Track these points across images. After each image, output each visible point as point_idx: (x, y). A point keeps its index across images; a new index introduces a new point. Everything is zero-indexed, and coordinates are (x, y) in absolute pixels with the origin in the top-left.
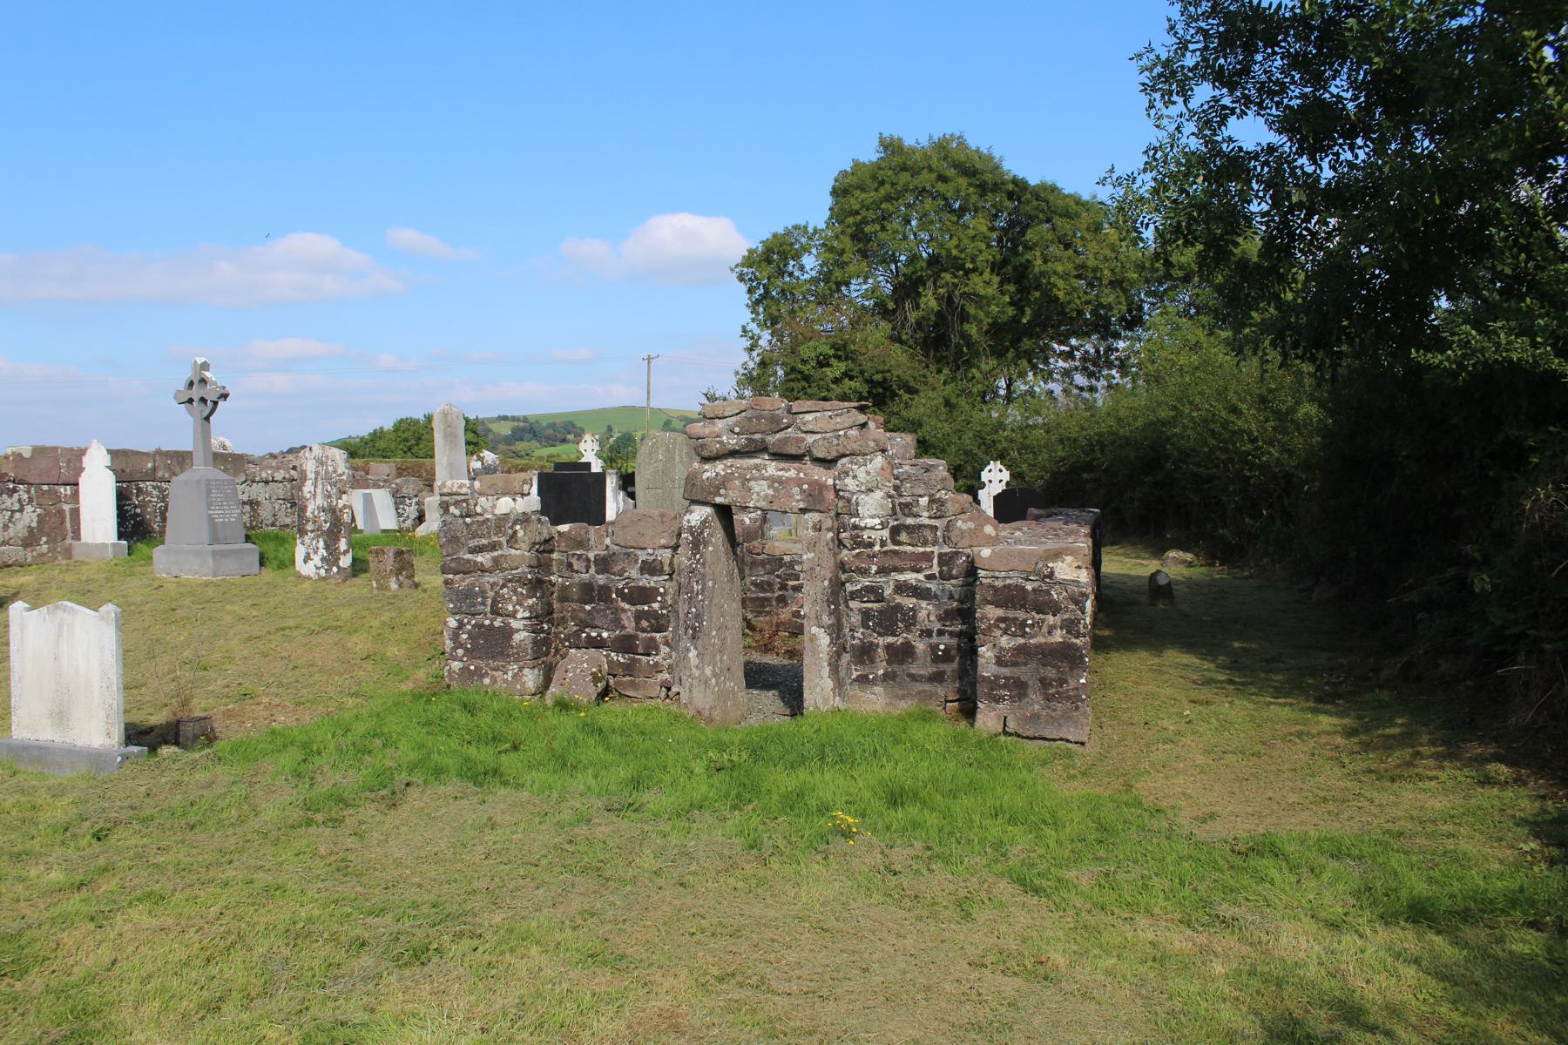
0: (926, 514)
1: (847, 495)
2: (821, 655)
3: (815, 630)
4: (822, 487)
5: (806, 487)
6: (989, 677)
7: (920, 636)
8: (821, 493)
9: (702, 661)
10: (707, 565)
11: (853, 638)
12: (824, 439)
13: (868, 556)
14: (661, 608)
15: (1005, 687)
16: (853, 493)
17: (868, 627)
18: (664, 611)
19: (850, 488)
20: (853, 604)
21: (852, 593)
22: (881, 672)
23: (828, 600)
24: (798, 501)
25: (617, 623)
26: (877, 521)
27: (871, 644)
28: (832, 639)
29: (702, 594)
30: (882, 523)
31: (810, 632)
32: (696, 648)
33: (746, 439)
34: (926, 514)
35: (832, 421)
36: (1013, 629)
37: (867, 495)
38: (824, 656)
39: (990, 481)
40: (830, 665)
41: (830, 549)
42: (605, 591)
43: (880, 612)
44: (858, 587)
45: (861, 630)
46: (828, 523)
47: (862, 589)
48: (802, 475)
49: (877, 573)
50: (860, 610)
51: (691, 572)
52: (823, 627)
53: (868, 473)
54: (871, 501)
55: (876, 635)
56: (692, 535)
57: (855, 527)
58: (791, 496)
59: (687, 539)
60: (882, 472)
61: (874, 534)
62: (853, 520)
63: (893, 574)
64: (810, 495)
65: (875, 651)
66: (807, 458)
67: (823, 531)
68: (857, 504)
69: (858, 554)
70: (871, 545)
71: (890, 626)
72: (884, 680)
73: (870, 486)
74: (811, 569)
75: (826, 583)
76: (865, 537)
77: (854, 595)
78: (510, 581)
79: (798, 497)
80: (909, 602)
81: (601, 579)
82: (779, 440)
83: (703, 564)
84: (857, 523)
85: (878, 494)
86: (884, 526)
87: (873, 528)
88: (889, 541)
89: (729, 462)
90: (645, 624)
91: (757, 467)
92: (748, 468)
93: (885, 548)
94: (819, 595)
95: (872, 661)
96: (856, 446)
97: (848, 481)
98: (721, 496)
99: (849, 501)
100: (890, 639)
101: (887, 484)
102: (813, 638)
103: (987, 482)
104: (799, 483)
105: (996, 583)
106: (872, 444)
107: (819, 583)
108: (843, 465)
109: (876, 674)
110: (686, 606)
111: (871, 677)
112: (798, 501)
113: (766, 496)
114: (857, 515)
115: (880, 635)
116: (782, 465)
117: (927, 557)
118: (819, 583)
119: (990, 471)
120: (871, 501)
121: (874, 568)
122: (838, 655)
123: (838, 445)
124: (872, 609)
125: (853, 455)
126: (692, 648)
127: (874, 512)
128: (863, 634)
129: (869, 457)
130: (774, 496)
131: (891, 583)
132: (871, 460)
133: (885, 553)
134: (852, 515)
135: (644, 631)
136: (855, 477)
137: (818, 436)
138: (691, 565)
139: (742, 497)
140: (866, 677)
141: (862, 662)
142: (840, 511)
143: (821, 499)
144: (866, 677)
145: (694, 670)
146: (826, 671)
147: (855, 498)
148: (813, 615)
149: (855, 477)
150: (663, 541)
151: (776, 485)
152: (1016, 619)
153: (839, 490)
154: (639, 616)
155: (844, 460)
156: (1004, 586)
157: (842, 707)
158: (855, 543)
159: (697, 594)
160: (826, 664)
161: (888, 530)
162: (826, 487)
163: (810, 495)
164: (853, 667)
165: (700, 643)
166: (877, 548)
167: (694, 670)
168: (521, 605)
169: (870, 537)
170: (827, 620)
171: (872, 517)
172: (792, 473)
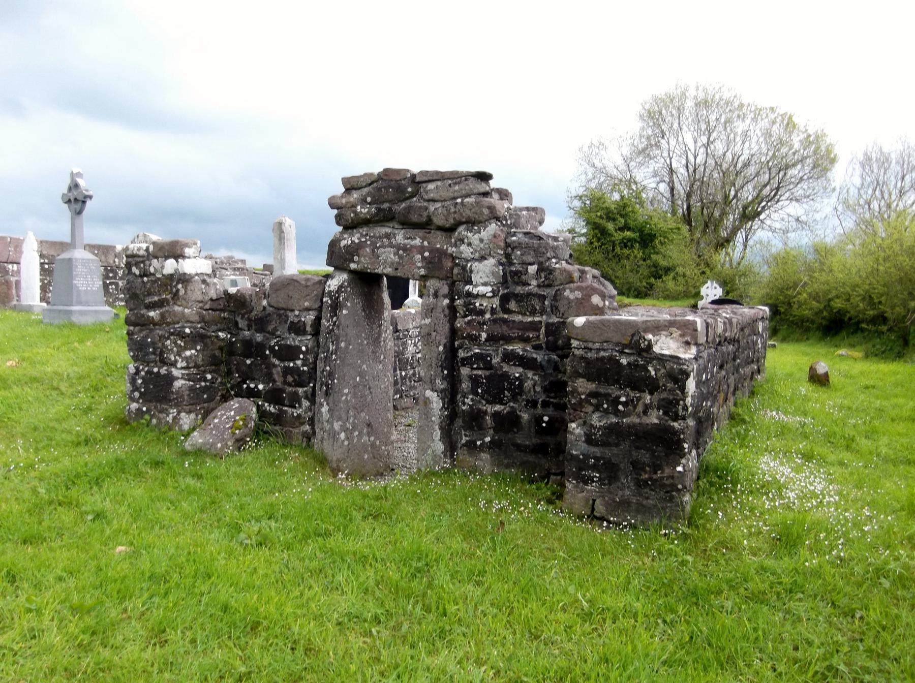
0: (534, 283)
5: (426, 254)
6: (578, 456)
7: (526, 406)
9: (332, 416)
10: (341, 327)
13: (479, 323)
14: (303, 365)
15: (594, 468)
17: (476, 394)
18: (305, 368)
20: (465, 371)
21: (463, 359)
22: (488, 439)
23: (441, 366)
25: (269, 378)
26: (489, 289)
27: (479, 410)
28: (444, 404)
29: (336, 354)
30: (493, 291)
32: (328, 404)
33: (376, 208)
34: (534, 283)
35: (451, 190)
36: (605, 406)
39: (708, 295)
40: (441, 428)
41: (445, 315)
42: (261, 346)
44: (469, 354)
46: (445, 290)
47: (472, 356)
48: (426, 243)
49: (486, 340)
51: (329, 333)
53: (481, 240)
55: (484, 402)
56: (331, 299)
57: (469, 294)
59: (327, 302)
60: (494, 240)
62: (467, 287)
65: (483, 418)
68: (471, 271)
69: (469, 322)
70: (482, 313)
75: (441, 348)
76: (477, 304)
77: (466, 362)
78: (172, 334)
79: (419, 265)
80: (517, 372)
81: (259, 337)
82: (405, 209)
83: (338, 326)
85: (491, 261)
86: (495, 293)
87: (484, 296)
89: (364, 231)
90: (290, 379)
91: (387, 236)
92: (381, 237)
93: (495, 316)
94: (434, 359)
97: (463, 248)
98: (354, 262)
100: (498, 408)
103: (704, 296)
104: (421, 250)
105: (589, 355)
107: (434, 348)
109: (484, 441)
110: (322, 365)
111: (478, 443)
112: (419, 268)
113: (392, 263)
114: (470, 282)
115: (488, 402)
116: (410, 232)
117: (535, 327)
118: (434, 348)
119: (708, 288)
121: (484, 336)
123: (455, 212)
124: (480, 376)
126: (325, 404)
127: (486, 279)
128: (472, 400)
130: (398, 263)
135: (290, 385)
136: (469, 244)
137: (438, 205)
138: (328, 327)
139: (372, 264)
142: (455, 278)
144: (474, 442)
145: (325, 424)
146: (437, 434)
150: (307, 304)
151: (401, 252)
152: (610, 395)
154: (286, 371)
156: (597, 359)
158: (467, 310)
159: (332, 354)
160: (437, 427)
165: (331, 398)
166: (488, 316)
167: (325, 424)
168: (180, 356)
171: (485, 284)
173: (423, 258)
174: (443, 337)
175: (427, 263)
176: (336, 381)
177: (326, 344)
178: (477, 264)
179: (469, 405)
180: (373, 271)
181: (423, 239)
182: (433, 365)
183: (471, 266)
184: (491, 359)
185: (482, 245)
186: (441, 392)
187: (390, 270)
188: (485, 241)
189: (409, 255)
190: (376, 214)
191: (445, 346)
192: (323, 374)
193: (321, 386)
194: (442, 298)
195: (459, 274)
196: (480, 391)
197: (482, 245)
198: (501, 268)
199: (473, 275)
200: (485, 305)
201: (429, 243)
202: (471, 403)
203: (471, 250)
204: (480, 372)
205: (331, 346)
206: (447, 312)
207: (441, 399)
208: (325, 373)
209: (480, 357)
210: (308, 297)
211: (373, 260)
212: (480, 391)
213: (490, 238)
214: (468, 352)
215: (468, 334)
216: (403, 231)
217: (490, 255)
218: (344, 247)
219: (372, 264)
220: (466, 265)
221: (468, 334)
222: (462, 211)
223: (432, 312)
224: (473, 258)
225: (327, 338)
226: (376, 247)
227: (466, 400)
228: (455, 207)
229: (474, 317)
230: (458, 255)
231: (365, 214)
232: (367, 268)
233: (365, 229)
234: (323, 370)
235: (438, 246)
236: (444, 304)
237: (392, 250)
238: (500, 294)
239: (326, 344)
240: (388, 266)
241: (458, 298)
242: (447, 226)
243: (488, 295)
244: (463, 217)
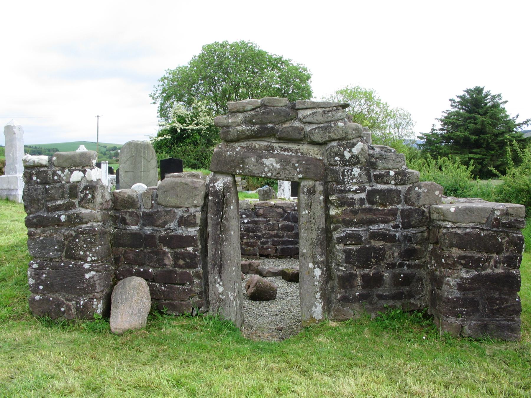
0: (393, 182)
6: (453, 299)
7: (387, 268)
15: (462, 306)
25: (160, 263)
27: (351, 274)
34: (393, 182)
35: (326, 116)
36: (470, 264)
46: (320, 188)
50: (345, 251)
65: (354, 279)
67: (317, 195)
77: (340, 240)
78: (82, 233)
80: (379, 244)
81: (148, 230)
90: (181, 262)
105: (459, 232)
115: (358, 267)
117: (394, 213)
135: (180, 267)
137: (315, 126)
152: (473, 257)
154: (176, 257)
156: (465, 234)
168: (90, 251)
204: (351, 247)
206: (323, 205)
209: (350, 236)
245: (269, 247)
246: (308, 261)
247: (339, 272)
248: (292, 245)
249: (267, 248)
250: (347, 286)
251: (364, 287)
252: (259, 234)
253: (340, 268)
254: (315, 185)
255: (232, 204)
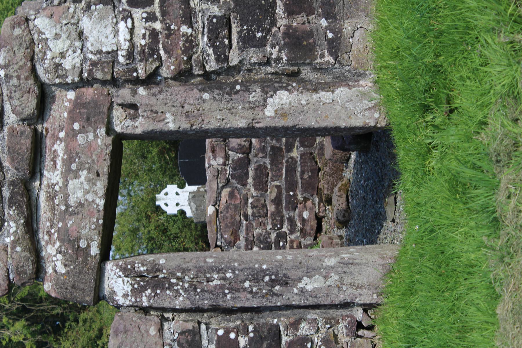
1: (86, 67)
2: (304, 102)
3: (269, 111)
4: (77, 104)
5: (76, 126)
8: (84, 105)
10: (184, 266)
11: (279, 60)
12: (10, 97)
13: (168, 36)
14: (246, 333)
16: (85, 58)
18: (251, 328)
19: (77, 61)
20: (234, 59)
21: (218, 60)
22: (324, 22)
23: (230, 94)
24: (96, 136)
26: (122, 25)
27: (286, 34)
28: (282, 88)
29: (225, 271)
30: (125, 19)
31: (273, 118)
32: (300, 280)
33: (10, 207)
37: (87, 39)
38: (304, 97)
39: (177, 204)
40: (316, 90)
41: (160, 92)
43: (242, 22)
44: (210, 51)
45: (268, 48)
47: (213, 46)
48: (62, 135)
49: (191, 26)
50: (242, 49)
51: (195, 289)
52: (265, 100)
53: (57, 37)
54: (95, 33)
55: (274, 29)
56: (143, 289)
57: (130, 55)
58: (90, 146)
59: (149, 298)
60: (56, 16)
61: (140, 31)
62: (121, 60)
63: (192, 5)
64: (88, 119)
65: (295, 30)
66: (39, 127)
67: (137, 100)
68: (99, 52)
69: (166, 51)
70: (154, 34)
71: (261, 9)
72: (334, 18)
73: (74, 35)
74: (188, 116)
75: (206, 96)
76: (143, 42)
79: (91, 136)
83: (184, 271)
84: (124, 53)
85: (86, 23)
86: (128, 16)
87: (131, 31)
88: (148, 9)
89: (43, 237)
91: (51, 198)
93: (158, 14)
94: (222, 106)
95: (310, 34)
96: (20, 53)
97: (67, 64)
98: (89, 246)
99: (94, 64)
100: (280, 10)
101: (71, 11)
102: (281, 113)
103: (179, 208)
104: (72, 134)
106: (18, 31)
107: (206, 106)
108: (46, 70)
109: (327, 28)
110: (242, 295)
111: (330, 35)
112: (96, 136)
113: (89, 180)
114: (114, 53)
115: (274, 23)
116: (48, 162)
118: (206, 106)
119: (166, 205)
120: (95, 33)
121: (185, 29)
122: (302, 82)
123: (19, 78)
124: (239, 33)
125: (32, 59)
126: (300, 285)
127: (110, 29)
128: (273, 46)
129: (36, 37)
130: (89, 170)
131: (204, 7)
132: (40, 33)
133: (164, 13)
134: (114, 62)
136: (62, 55)
138: (185, 290)
139: (91, 215)
140: (330, 42)
141: (311, 50)
142: (108, 77)
143: (95, 104)
144: (330, 42)
145: (330, 282)
146: (325, 96)
147: (90, 56)
148: (250, 114)
149: (62, 55)
150: (153, 331)
151: (74, 167)
153: (81, 79)
155: (40, 71)
157: (373, 76)
158: (152, 55)
159: (225, 279)
160: (315, 96)
161: (134, 10)
162: (77, 98)
163: (88, 119)
164: (318, 60)
165: (292, 274)
166: (158, 26)
167: (330, 282)
169: (144, 36)
170: (255, 96)
171: (116, 32)
172: (60, 148)
173: (83, 130)
174: (191, 94)
175: (89, 125)
176: (265, 267)
177: (210, 292)
178: (88, 45)
179: (280, 51)
180: (102, 213)
181: (56, 138)
182: (229, 106)
183: (91, 52)
184: (215, 17)
185: (64, 36)
186: (267, 93)
187: (99, 184)
188: (58, 31)
189: (77, 154)
190: (19, 207)
191: (202, 90)
192: (256, 293)
193: (274, 294)
194: (137, 97)
195: (103, 70)
196: (259, 35)
197: (64, 36)
198: (93, 7)
199: (104, 50)
200: (143, 31)
201: (62, 130)
202: (277, 47)
203: (70, 52)
204: (235, 36)
205: (215, 283)
206: (155, 89)
207: (275, 93)
208: (255, 289)
209: (213, 37)
210: (142, 328)
211: (85, 212)
212: (259, 35)
213: (53, 23)
214: (208, 55)
215: (183, 52)
216: (46, 173)
217: (77, 24)
218: (65, 265)
219: (91, 215)
220: (90, 60)
221: (183, 52)
222: (16, 67)
223: (157, 112)
224: (82, 50)
225: (203, 290)
226: (67, 210)
227: (274, 56)
228: (11, 77)
229: (161, 46)
230: (78, 71)
231: (17, 227)
232: (97, 225)
233: (41, 236)
234: (251, 292)
235: (66, 114)
236: (144, 93)
237: (70, 182)
238: (128, 8)
239: (210, 292)
240: (94, 188)
241: (136, 70)
242: (36, 91)
243: (130, 25)
244: (25, 64)
245: (300, 215)
246: (261, 116)
247: (282, 59)
248: (294, 170)
249: (303, 221)
250: (310, 44)
251: (310, 12)
252: (273, 236)
253: (274, 56)
254: (119, 105)
255: (157, 262)
